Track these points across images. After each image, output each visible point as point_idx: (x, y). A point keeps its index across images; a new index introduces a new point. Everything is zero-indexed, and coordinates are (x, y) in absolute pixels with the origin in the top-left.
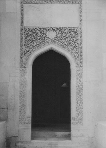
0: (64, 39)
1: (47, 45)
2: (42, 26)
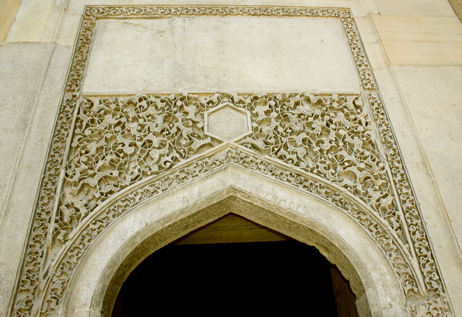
1: (202, 175)
2: (180, 90)
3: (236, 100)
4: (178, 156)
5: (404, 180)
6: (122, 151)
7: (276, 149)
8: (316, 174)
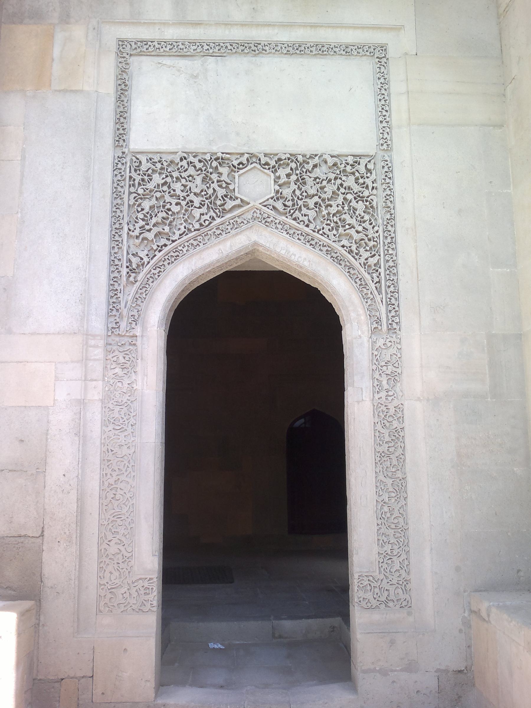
0: (312, 206)
1: (233, 232)
2: (214, 149)
3: (263, 162)
4: (214, 215)
5: (393, 242)
6: (169, 210)
7: (292, 211)
8: (322, 235)
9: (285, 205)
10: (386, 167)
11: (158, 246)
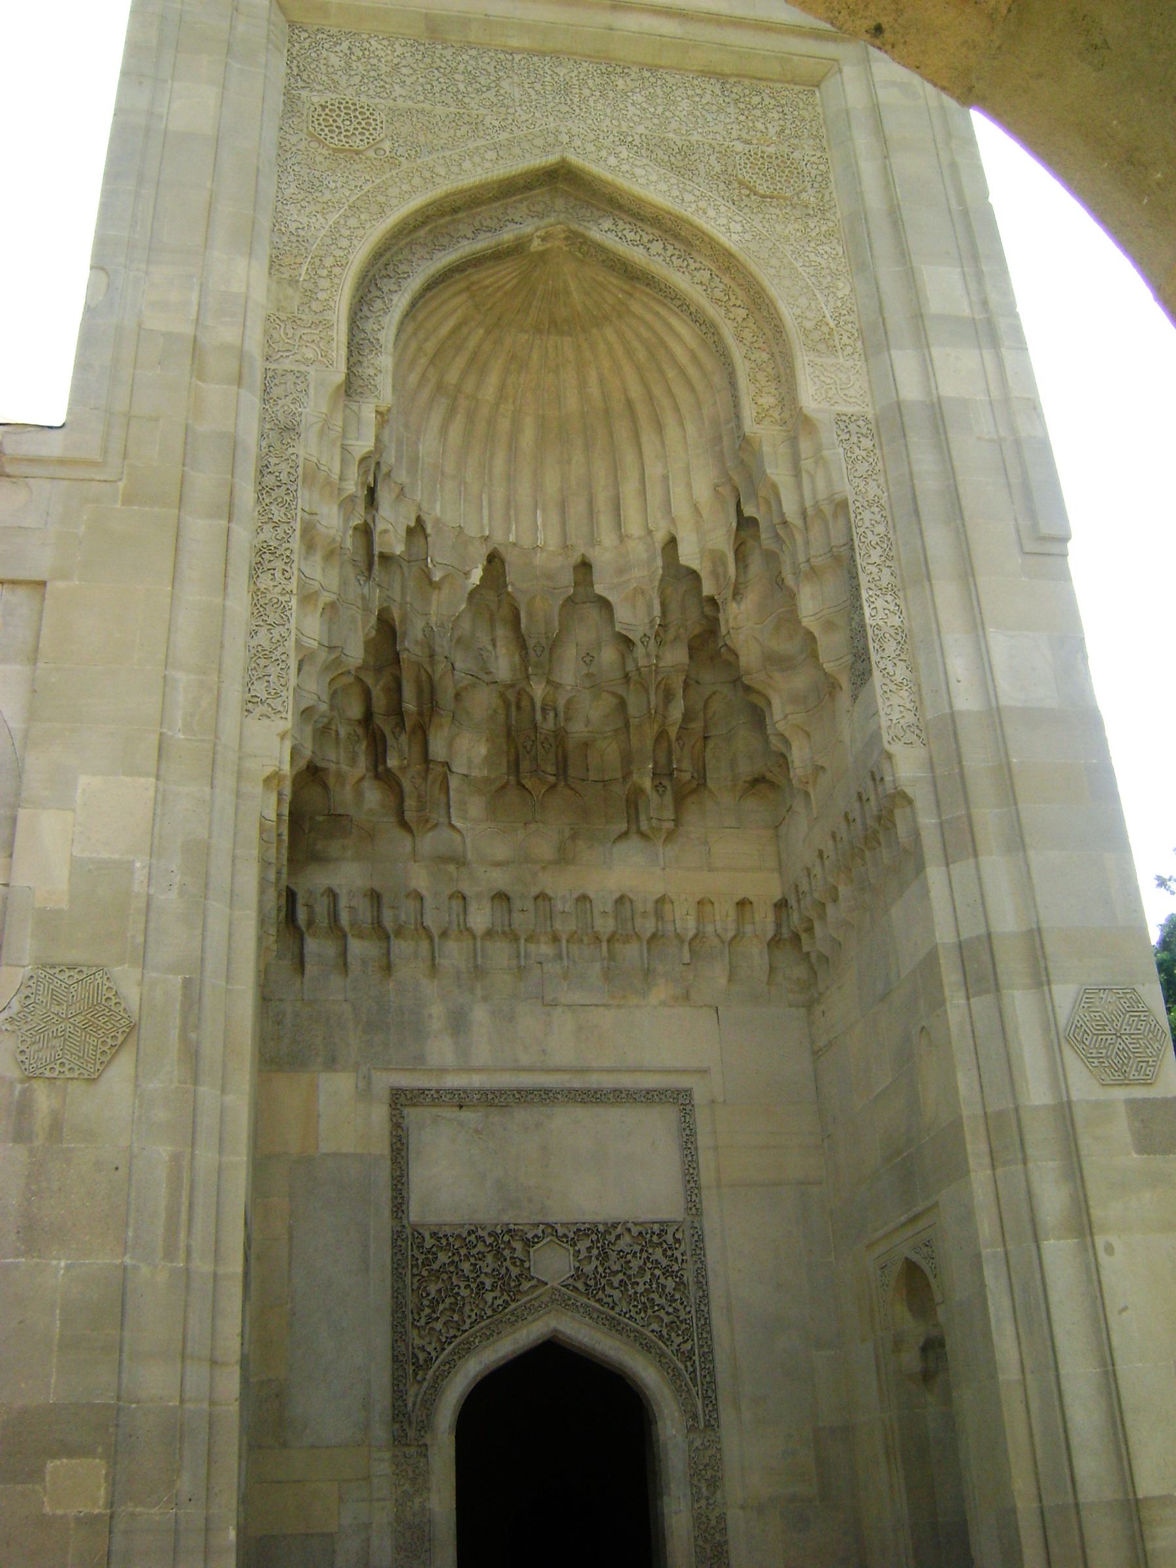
0: (616, 1284)
1: (530, 1318)
2: (505, 1219)
3: (560, 1234)
4: (509, 1299)
6: (458, 1294)
9: (586, 1284)
10: (696, 1236)
11: (447, 1338)
